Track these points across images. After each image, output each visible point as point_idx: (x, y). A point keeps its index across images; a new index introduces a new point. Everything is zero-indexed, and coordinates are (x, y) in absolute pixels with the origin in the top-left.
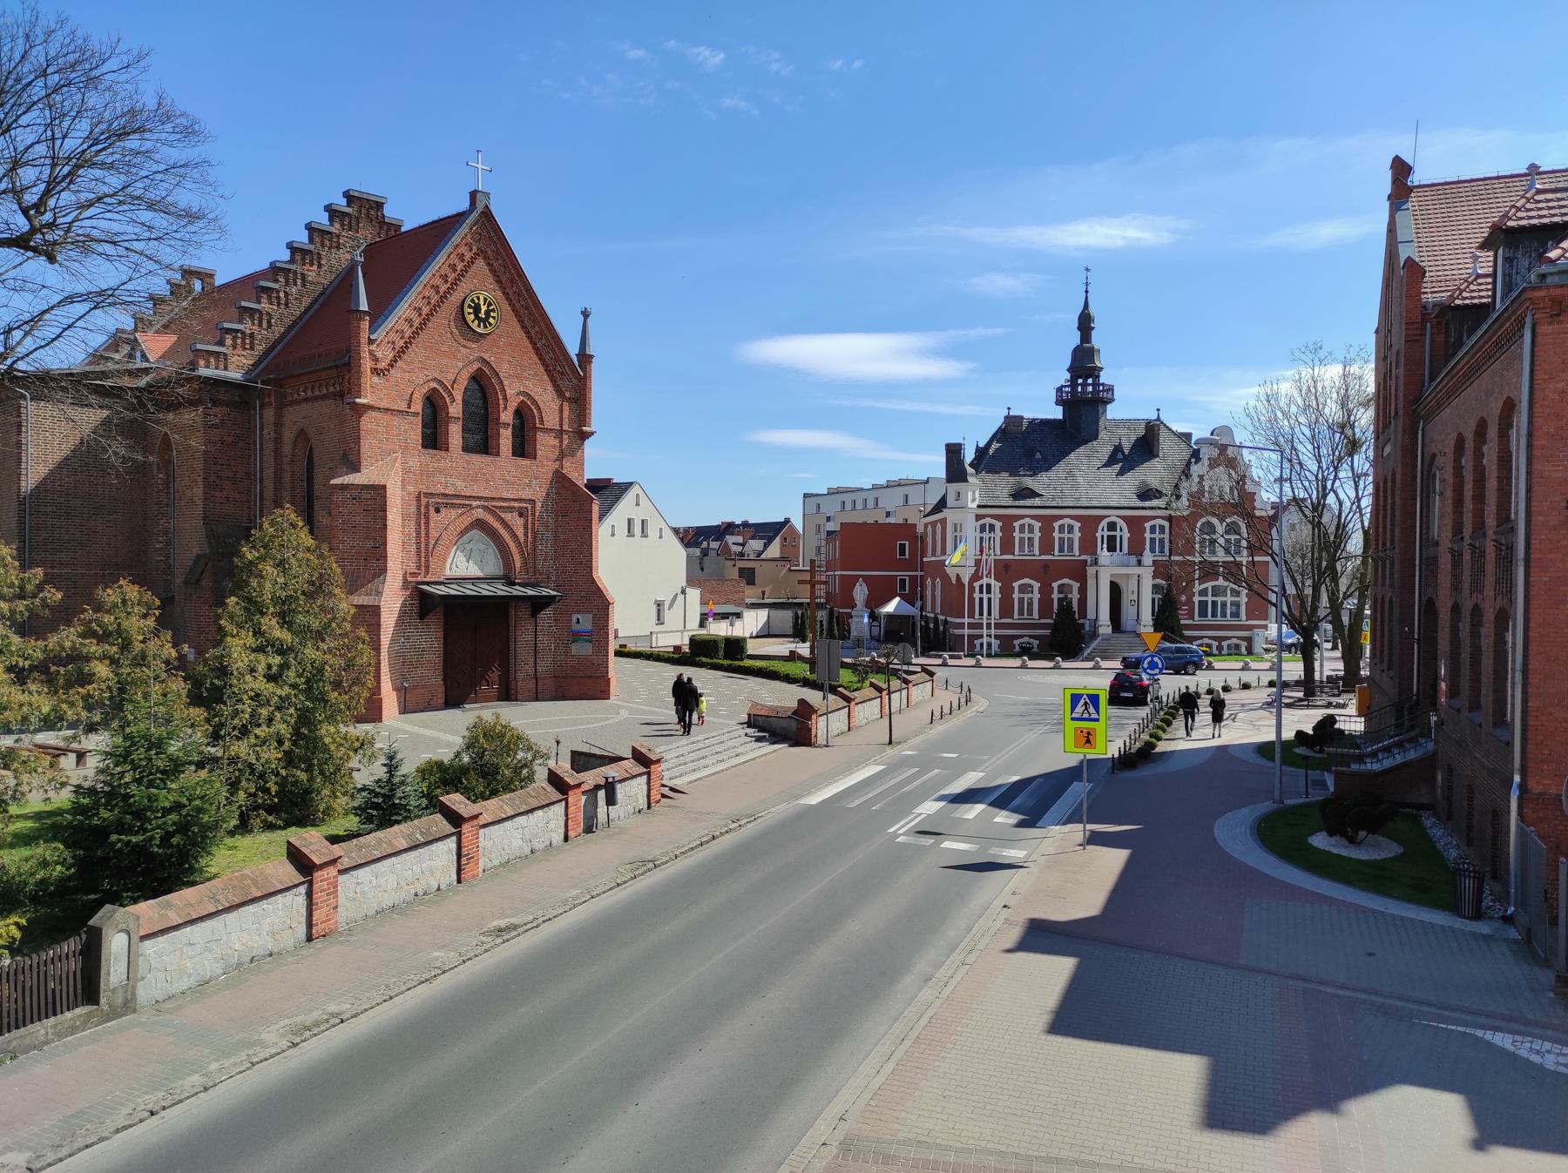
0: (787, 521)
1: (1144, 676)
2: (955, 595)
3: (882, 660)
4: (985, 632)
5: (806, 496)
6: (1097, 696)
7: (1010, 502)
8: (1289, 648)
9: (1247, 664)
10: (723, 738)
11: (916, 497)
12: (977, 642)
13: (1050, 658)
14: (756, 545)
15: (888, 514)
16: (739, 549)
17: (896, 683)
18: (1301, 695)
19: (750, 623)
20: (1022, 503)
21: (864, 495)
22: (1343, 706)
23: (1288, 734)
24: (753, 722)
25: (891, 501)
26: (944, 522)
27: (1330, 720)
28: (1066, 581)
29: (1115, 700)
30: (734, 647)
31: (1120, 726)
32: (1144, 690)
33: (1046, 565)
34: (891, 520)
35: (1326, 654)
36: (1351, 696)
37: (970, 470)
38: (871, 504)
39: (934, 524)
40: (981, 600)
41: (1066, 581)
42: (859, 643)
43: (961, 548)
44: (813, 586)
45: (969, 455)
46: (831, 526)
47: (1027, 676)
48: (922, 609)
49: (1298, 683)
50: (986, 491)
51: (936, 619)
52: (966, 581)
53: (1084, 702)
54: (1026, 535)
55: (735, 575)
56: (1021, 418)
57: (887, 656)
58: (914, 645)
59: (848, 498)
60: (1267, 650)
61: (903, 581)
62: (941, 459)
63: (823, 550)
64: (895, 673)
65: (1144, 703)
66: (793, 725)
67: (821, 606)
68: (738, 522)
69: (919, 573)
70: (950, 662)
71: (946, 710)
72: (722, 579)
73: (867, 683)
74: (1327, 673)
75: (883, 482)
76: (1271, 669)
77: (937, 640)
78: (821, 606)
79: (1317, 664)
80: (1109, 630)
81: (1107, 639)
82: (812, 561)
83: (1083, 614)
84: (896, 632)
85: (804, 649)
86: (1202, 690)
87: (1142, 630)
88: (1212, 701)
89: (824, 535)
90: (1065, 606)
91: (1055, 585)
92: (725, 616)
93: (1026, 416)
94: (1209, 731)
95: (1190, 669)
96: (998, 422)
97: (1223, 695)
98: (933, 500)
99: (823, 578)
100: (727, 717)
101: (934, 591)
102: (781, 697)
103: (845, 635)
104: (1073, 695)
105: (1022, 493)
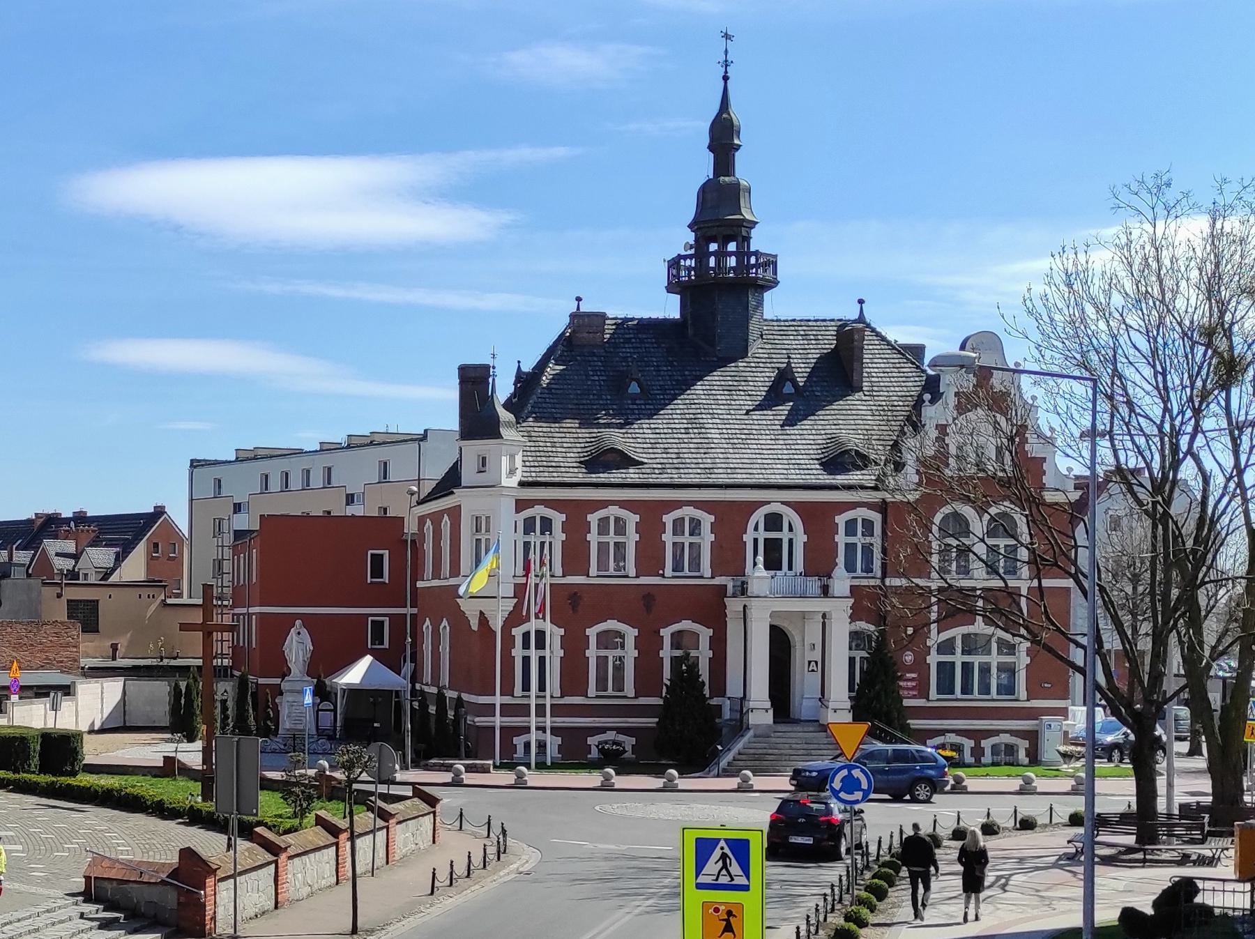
0: (159, 512)
1: (835, 805)
2: (478, 651)
3: (339, 775)
4: (533, 721)
5: (195, 464)
6: (746, 843)
7: (580, 476)
8: (1108, 751)
9: (1028, 781)
10: (39, 922)
11: (403, 465)
12: (519, 741)
13: (656, 770)
14: (101, 556)
15: (350, 499)
16: (68, 564)
17: (364, 819)
18: (1131, 840)
19: (90, 704)
20: (603, 477)
21: (304, 463)
22: (1211, 862)
23: (1107, 915)
24: (94, 891)
25: (356, 474)
26: (455, 513)
27: (1186, 888)
28: (686, 625)
29: (779, 850)
30: (60, 750)
31: (789, 900)
32: (836, 832)
33: (648, 596)
34: (357, 510)
35: (1179, 764)
36: (1226, 842)
37: (505, 415)
38: (317, 480)
39: (436, 518)
40: (526, 660)
41: (686, 625)
42: (295, 742)
43: (488, 562)
44: (208, 635)
45: (503, 388)
46: (242, 522)
47: (613, 806)
48: (415, 678)
49: (1125, 818)
50: (535, 456)
51: (440, 698)
52: (497, 624)
53: (720, 855)
54: (612, 538)
55: (63, 616)
56: (602, 317)
57: (348, 766)
58: (400, 746)
59: (275, 469)
60: (1066, 756)
61: (378, 626)
62: (451, 394)
63: (227, 566)
64: (363, 799)
65: (834, 856)
66: (171, 898)
67: (223, 673)
68: (67, 513)
69: (409, 610)
70: (468, 778)
71: (460, 869)
72: (37, 622)
73: (311, 818)
74: (1179, 799)
75: (340, 437)
76: (1074, 792)
77: (443, 737)
78: (223, 673)
79: (1161, 783)
80: (768, 718)
81: (763, 735)
82: (207, 588)
83: (719, 684)
84: (365, 720)
85: (191, 754)
86: (944, 831)
87: (831, 718)
88: (963, 851)
89: (228, 539)
90: (685, 673)
91: (666, 633)
92: (41, 692)
93: (610, 314)
94: (957, 909)
95: (922, 792)
96: (558, 325)
97: (983, 841)
98: (435, 472)
99: (227, 620)
100: (46, 882)
101: (437, 643)
102: (147, 844)
103: (268, 727)
104: (699, 841)
105: (604, 460)
